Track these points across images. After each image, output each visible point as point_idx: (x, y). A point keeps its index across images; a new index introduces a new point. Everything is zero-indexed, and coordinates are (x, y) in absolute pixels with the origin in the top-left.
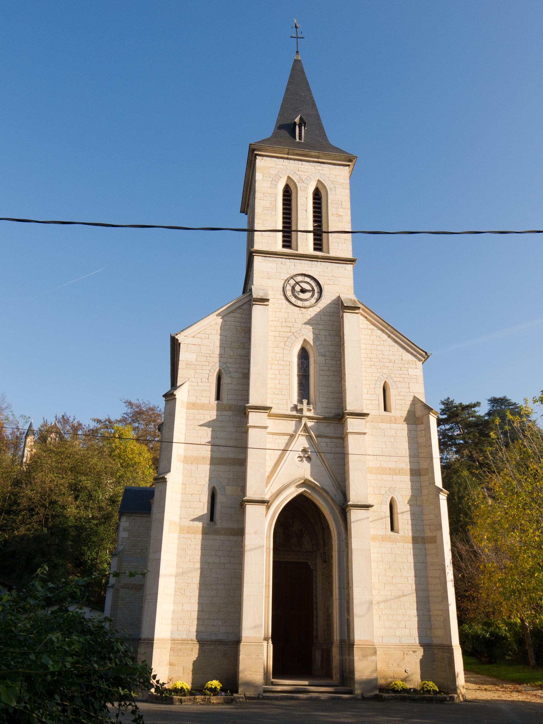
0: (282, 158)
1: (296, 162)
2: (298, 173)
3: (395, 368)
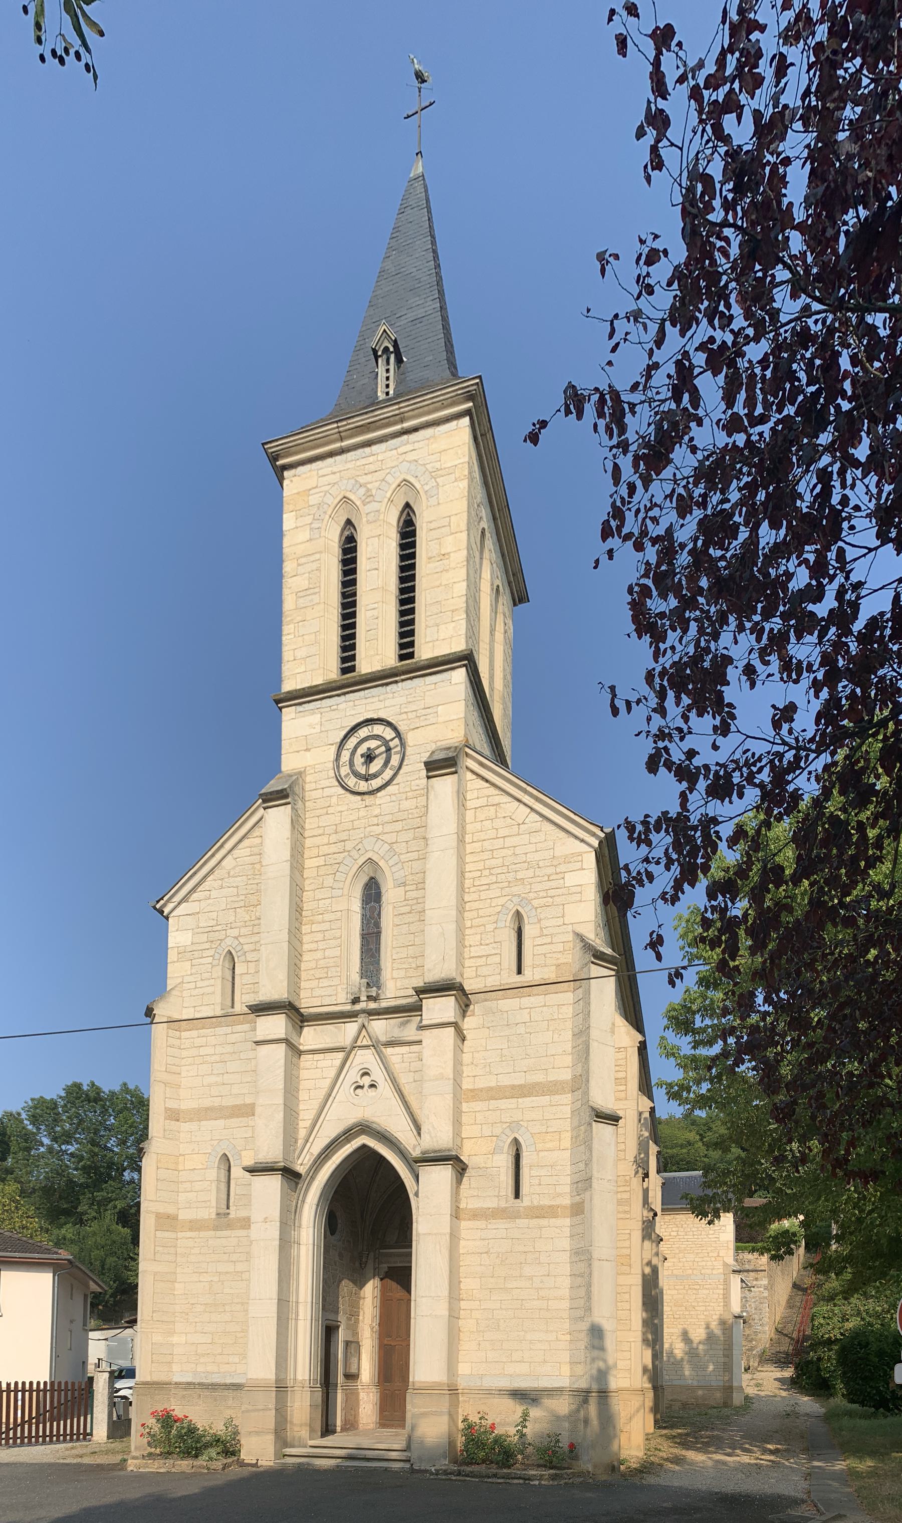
1: (360, 451)
2: (362, 480)
3: (539, 879)
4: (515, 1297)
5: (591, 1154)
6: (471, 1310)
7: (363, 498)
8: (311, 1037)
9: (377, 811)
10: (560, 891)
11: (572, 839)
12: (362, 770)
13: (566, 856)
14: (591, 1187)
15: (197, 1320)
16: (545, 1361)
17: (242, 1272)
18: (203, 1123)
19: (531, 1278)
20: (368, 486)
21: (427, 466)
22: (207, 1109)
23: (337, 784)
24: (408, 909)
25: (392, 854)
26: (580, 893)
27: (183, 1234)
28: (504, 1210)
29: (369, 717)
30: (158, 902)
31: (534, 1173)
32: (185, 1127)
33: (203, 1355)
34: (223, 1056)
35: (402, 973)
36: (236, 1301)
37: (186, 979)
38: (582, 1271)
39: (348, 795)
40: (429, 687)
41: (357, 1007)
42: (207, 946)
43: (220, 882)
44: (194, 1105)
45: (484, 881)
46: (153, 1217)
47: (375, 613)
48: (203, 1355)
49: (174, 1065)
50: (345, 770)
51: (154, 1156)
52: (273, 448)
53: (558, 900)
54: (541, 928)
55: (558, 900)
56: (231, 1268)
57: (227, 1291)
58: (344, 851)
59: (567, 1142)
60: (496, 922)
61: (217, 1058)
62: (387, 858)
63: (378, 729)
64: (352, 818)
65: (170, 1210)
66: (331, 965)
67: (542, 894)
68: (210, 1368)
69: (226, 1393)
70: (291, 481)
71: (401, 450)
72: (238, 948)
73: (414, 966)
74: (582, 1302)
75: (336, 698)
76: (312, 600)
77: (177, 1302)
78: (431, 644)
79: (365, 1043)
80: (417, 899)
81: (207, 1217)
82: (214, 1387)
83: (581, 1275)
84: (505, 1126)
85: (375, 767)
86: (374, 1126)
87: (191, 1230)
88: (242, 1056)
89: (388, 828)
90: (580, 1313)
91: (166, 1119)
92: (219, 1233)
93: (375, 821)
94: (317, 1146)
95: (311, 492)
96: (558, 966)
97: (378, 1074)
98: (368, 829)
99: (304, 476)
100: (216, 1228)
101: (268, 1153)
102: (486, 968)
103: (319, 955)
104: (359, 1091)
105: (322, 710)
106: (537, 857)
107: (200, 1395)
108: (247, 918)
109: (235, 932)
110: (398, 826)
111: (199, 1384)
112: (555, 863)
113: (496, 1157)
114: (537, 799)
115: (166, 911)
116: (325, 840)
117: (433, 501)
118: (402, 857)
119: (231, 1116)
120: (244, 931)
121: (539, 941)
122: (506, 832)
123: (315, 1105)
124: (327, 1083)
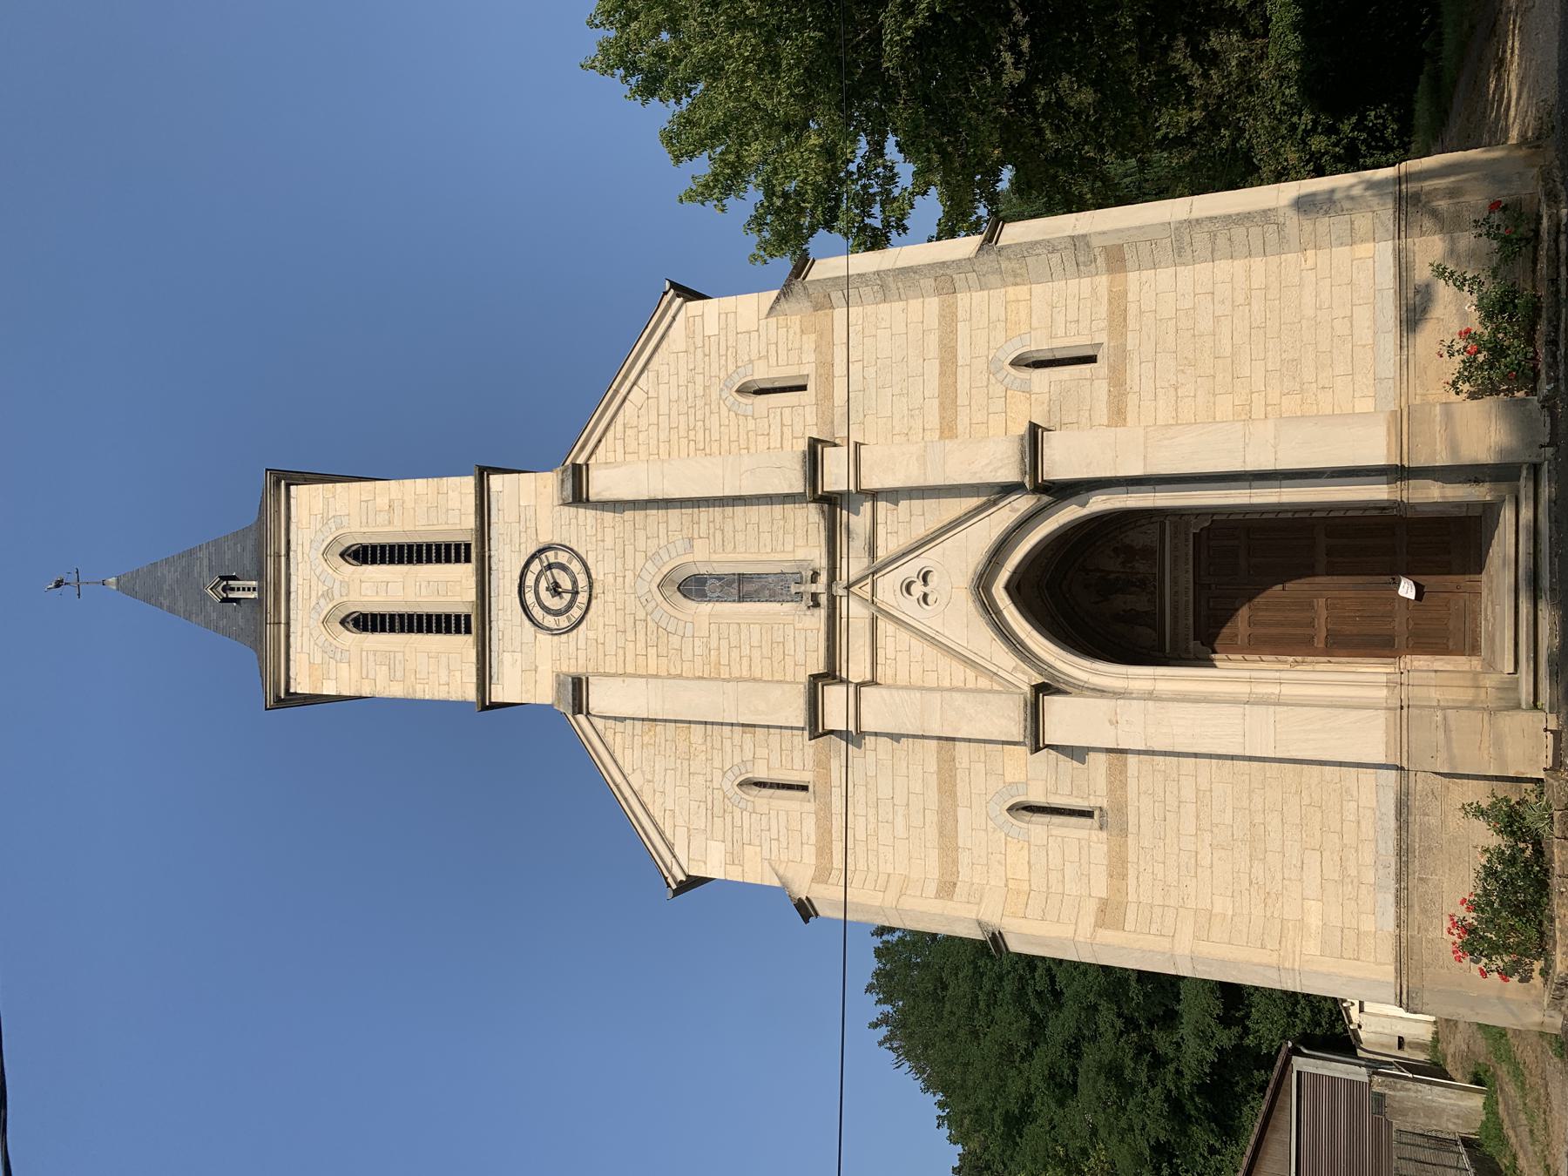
0: (288, 637)
5: (1036, 243)
8: (858, 669)
9: (610, 578)
10: (723, 339)
12: (567, 597)
14: (1084, 236)
15: (1279, 876)
17: (1198, 790)
19: (1216, 319)
22: (941, 834)
24: (718, 534)
32: (964, 873)
33: (1343, 868)
35: (789, 538)
36: (1245, 803)
37: (766, 855)
38: (1206, 236)
39: (588, 616)
41: (823, 599)
42: (728, 818)
44: (934, 854)
45: (700, 436)
47: (424, 584)
48: (1343, 868)
50: (563, 622)
51: (1006, 921)
59: (1022, 291)
61: (872, 811)
63: (530, 580)
64: (613, 611)
65: (1091, 907)
68: (1368, 858)
69: (1415, 828)
74: (1255, 231)
77: (1245, 912)
79: (868, 588)
81: (1105, 847)
82: (1404, 853)
83: (1213, 236)
85: (566, 583)
87: (1124, 876)
89: (630, 564)
90: (1272, 237)
92: (1132, 828)
93: (620, 580)
94: (1003, 658)
97: (910, 569)
100: (1124, 832)
102: (796, 420)
103: (756, 654)
104: (930, 599)
106: (683, 372)
107: (1421, 879)
110: (629, 549)
111: (1399, 881)
113: (1035, 389)
114: (625, 377)
115: (681, 877)
117: (345, 520)
119: (953, 794)
120: (717, 764)
121: (773, 361)
123: (945, 662)
124: (917, 645)
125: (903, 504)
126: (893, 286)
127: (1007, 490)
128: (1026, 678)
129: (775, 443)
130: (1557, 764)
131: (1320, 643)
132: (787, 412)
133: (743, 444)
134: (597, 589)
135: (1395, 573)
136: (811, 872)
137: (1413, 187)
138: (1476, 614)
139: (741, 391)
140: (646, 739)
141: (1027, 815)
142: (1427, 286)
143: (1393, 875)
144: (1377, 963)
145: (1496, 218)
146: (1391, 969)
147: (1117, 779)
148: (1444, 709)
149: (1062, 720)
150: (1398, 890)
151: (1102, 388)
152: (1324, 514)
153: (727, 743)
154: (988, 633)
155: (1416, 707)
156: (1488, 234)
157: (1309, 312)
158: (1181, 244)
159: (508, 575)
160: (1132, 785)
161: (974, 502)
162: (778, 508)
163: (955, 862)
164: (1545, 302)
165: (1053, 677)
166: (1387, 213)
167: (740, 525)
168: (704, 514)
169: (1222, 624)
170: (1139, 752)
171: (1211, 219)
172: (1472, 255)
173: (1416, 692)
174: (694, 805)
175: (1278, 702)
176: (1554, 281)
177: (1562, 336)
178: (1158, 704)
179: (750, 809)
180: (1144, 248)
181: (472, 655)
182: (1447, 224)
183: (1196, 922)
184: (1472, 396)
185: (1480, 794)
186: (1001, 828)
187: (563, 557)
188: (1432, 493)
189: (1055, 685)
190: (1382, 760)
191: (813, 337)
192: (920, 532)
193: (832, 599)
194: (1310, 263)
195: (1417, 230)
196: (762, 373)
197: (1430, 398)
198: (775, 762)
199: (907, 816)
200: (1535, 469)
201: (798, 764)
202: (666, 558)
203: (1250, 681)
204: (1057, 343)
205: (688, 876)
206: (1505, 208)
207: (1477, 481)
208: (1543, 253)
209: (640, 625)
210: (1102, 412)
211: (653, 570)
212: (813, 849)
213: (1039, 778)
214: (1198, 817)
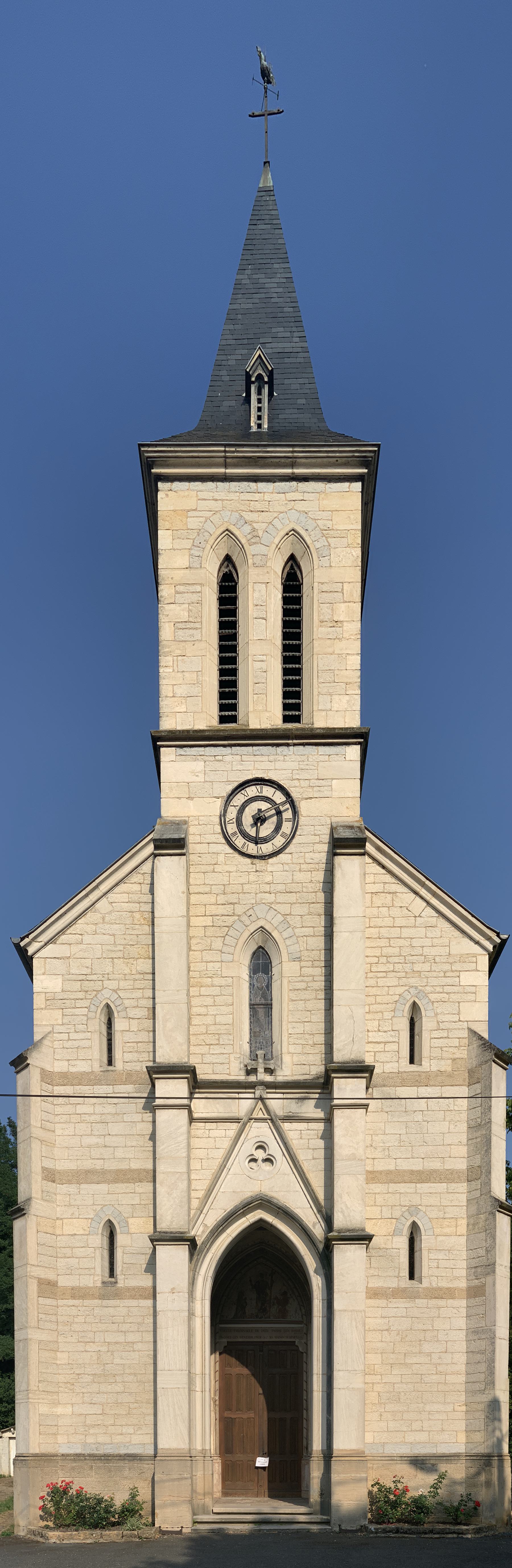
1: (244, 484)
2: (248, 516)
3: (435, 974)
4: (415, 1372)
6: (373, 1384)
7: (249, 537)
8: (202, 1107)
9: (269, 878)
10: (456, 989)
11: (467, 940)
12: (252, 832)
13: (461, 956)
14: (494, 1272)
15: (84, 1390)
16: (443, 1430)
17: (133, 1343)
18: (83, 1186)
19: (429, 1354)
20: (254, 525)
21: (319, 522)
22: (88, 1172)
23: (224, 841)
24: (303, 985)
25: (286, 926)
26: (475, 993)
27: (65, 1302)
28: (404, 1290)
29: (260, 776)
30: (22, 939)
31: (432, 1256)
32: (63, 1188)
33: (93, 1426)
34: (104, 1117)
35: (299, 1049)
36: (127, 1371)
37: (58, 1029)
39: (237, 855)
40: (322, 758)
41: (252, 1078)
42: (81, 995)
43: (94, 927)
44: (72, 1166)
45: (382, 968)
46: (35, 1282)
48: (93, 1426)
49: (48, 1121)
50: (232, 828)
52: (150, 452)
53: (454, 997)
54: (438, 1022)
55: (454, 997)
56: (121, 1338)
57: (117, 1361)
58: (234, 915)
59: (463, 1228)
60: (394, 1011)
62: (281, 929)
63: (268, 791)
66: (223, 1032)
67: (438, 989)
68: (101, 1439)
69: (121, 1464)
70: (167, 495)
71: (291, 496)
72: (118, 1002)
73: (311, 1042)
74: (482, 1376)
75: (221, 748)
76: (193, 635)
77: (60, 1371)
78: (324, 713)
79: (261, 1115)
80: (313, 976)
81: (91, 1285)
82: (106, 1458)
84: (404, 1209)
85: (266, 830)
86: (275, 1201)
87: (73, 1297)
88: (126, 1118)
90: (477, 1387)
91: (43, 1179)
92: (106, 1302)
94: (212, 1218)
95: (190, 514)
96: (454, 1060)
97: (275, 1149)
98: (259, 895)
99: (180, 493)
100: (102, 1297)
101: (172, 1222)
105: (206, 758)
106: (434, 951)
107: (92, 1467)
108: (127, 971)
109: (113, 985)
110: (292, 898)
112: (451, 960)
113: (396, 1239)
114: (434, 894)
115: (31, 950)
116: (213, 900)
117: (325, 561)
118: (296, 930)
119: (116, 1181)
120: (123, 984)
121: (436, 1034)
122: (403, 922)
123: (208, 1175)
124: (220, 1154)
125: (321, 1143)
126: (479, 1134)
127: (328, 1220)
128: (200, 1232)
129: (373, 1036)
130: (164, 1533)
131: (227, 1414)
132: (394, 1047)
133: (374, 1008)
134: (260, 864)
135: (268, 1454)
136: (48, 1068)
137: (495, 1463)
138: (246, 1495)
139: (415, 1007)
140: (137, 916)
141: (107, 1234)
142: (436, 1470)
143: (92, 1452)
144: (39, 1444)
145: (471, 1505)
146: (37, 1451)
147: (136, 1293)
148: (191, 1478)
149: (173, 1257)
150: (84, 1455)
151: (393, 1284)
152: (305, 1416)
153: (139, 994)
154: (230, 1206)
155: (192, 1464)
156: (462, 1501)
157: (428, 1408)
158: (480, 1333)
159: (271, 766)
160: (134, 1303)
161: (321, 1196)
162: (321, 1039)
163: (69, 1182)
164: (420, 1528)
165: (201, 1251)
166: (482, 1449)
167: (310, 1005)
168: (319, 972)
169: (238, 1358)
170: (155, 1307)
171: (494, 1351)
172: (452, 1493)
173: (200, 1465)
174: (88, 962)
175: (191, 1390)
176: (431, 1532)
177: (401, 1535)
178: (186, 1318)
179: (91, 1015)
180: (481, 1310)
181: (201, 725)
182: (471, 1481)
183: (50, 1342)
184: (370, 1493)
185: (144, 1495)
186: (97, 1215)
187: (287, 827)
188: (315, 1472)
189: (196, 1253)
190: (160, 1446)
191: (449, 1069)
192: (301, 1156)
193: (252, 1086)
194: (457, 1408)
195: (469, 1465)
196: (427, 1024)
197: (370, 1471)
198: (128, 1037)
199: (97, 1146)
200: (328, 1523)
201: (128, 1057)
202: (285, 935)
203: (203, 1374)
204: (425, 1253)
205: (31, 958)
206: (475, 1509)
207: (322, 1495)
208: (448, 1526)
209: (229, 909)
210: (375, 1283)
211: (275, 922)
212: (65, 1070)
213: (133, 1241)
214: (116, 1343)
